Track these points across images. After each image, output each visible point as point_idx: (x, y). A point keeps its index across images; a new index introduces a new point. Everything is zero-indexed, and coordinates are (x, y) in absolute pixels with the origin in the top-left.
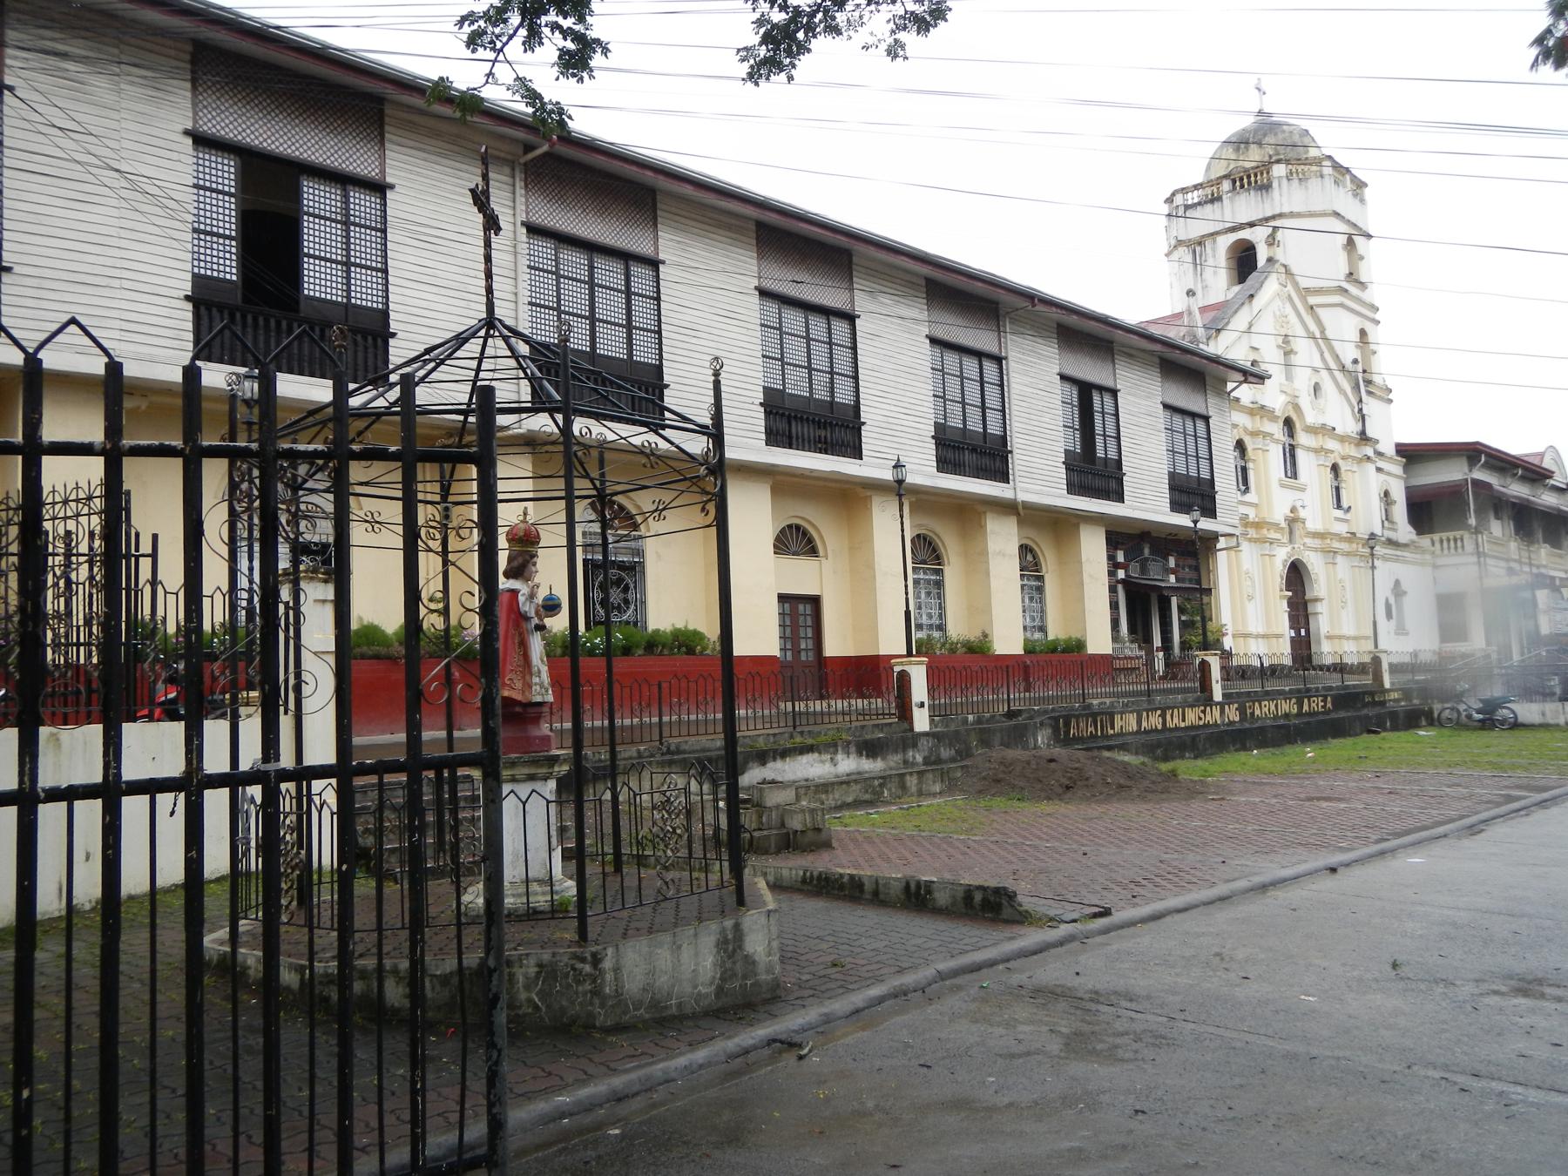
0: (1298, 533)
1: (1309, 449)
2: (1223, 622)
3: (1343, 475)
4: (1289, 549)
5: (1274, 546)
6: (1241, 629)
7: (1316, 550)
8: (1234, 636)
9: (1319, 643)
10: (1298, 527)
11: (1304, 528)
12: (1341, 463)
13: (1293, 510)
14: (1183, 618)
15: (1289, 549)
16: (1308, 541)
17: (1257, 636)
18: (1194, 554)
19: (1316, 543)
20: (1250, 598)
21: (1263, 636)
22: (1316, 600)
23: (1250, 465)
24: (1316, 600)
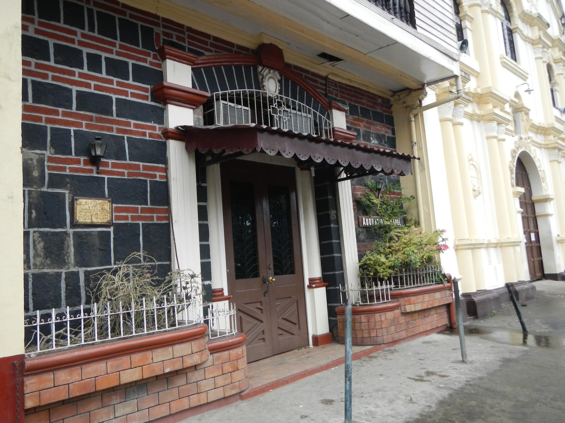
0: (523, 125)
1: (526, 39)
2: (439, 227)
3: (557, 78)
4: (516, 138)
5: (503, 128)
6: (467, 236)
7: (540, 146)
8: (457, 248)
9: (551, 248)
10: (522, 115)
11: (528, 120)
12: (553, 65)
13: (517, 95)
14: (367, 221)
15: (516, 138)
16: (531, 134)
17: (488, 246)
18: (390, 121)
19: (539, 139)
20: (477, 193)
21: (498, 245)
22: (546, 200)
23: (466, 24)
24: (546, 200)
